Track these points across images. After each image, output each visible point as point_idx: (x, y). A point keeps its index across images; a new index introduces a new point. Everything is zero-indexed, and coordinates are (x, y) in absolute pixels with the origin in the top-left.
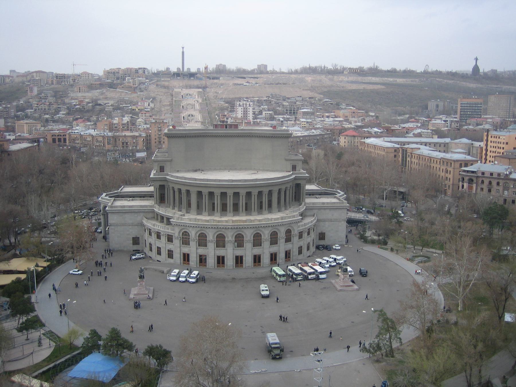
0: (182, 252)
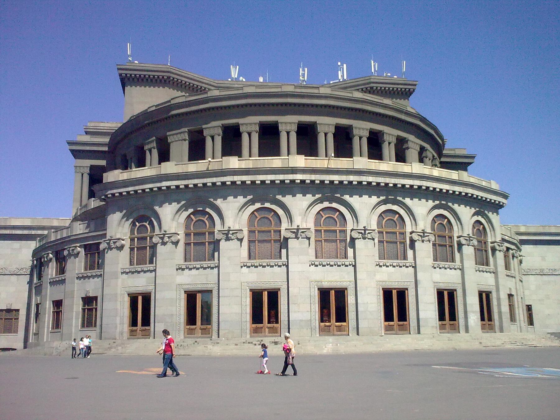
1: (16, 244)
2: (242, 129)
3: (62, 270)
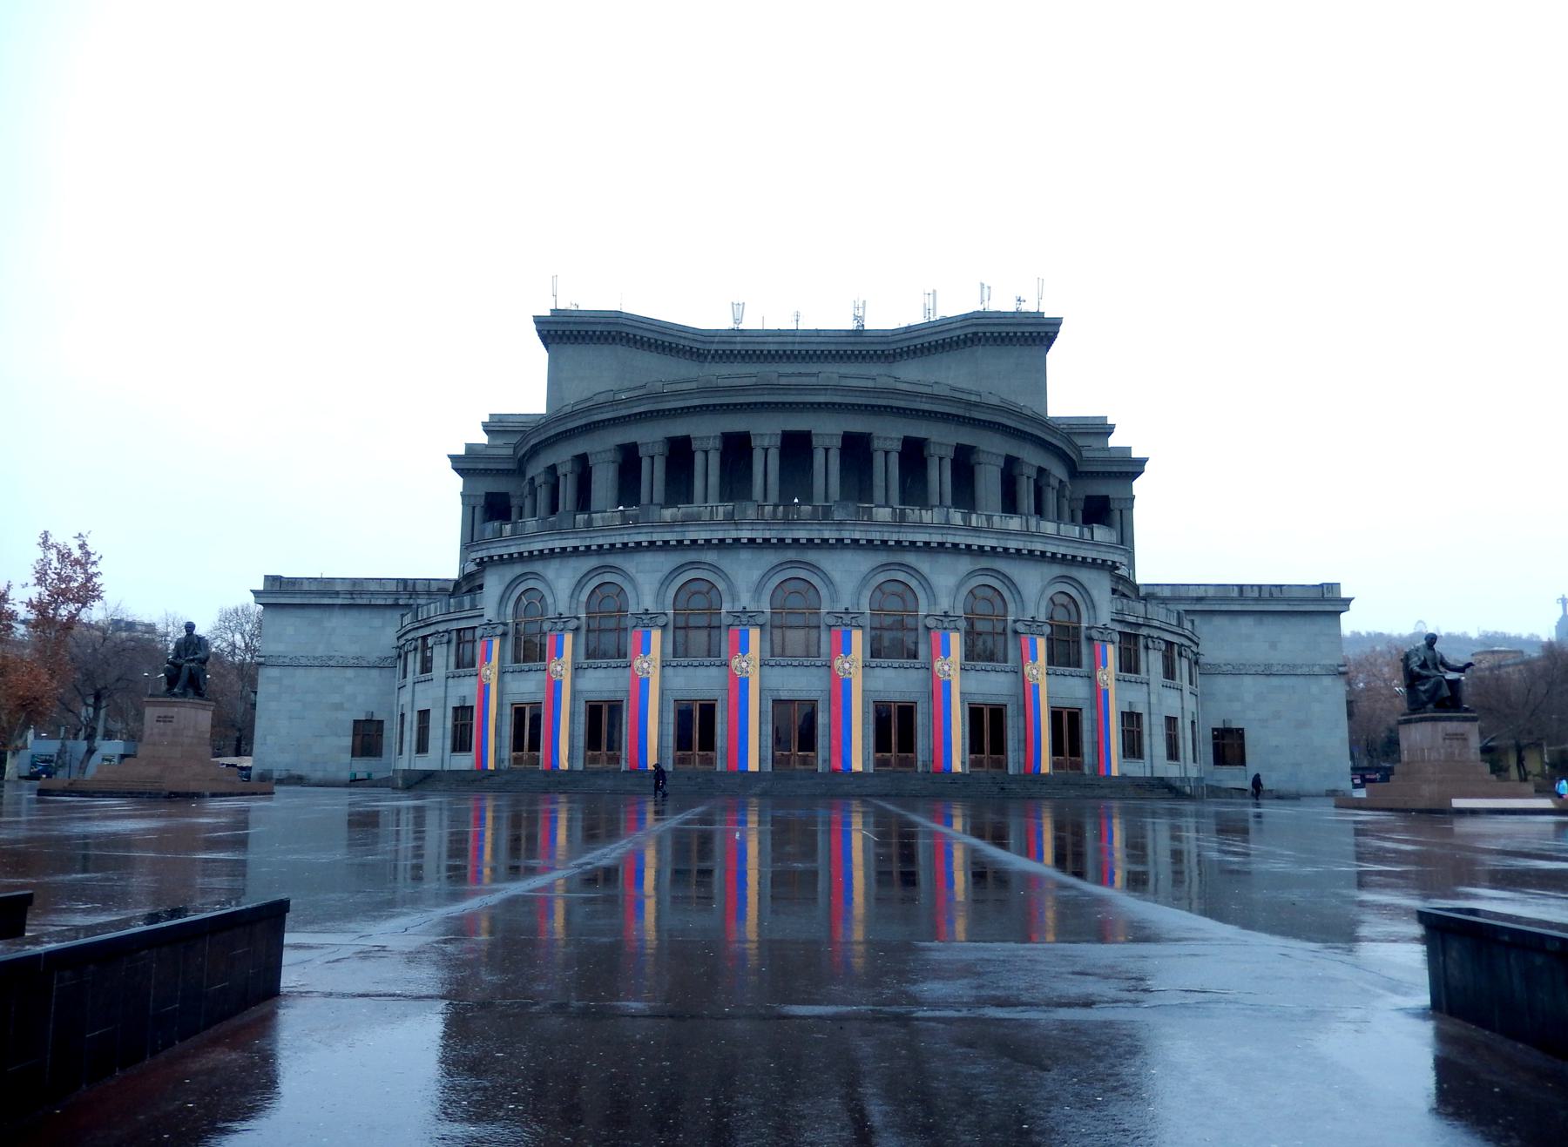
0: (508, 700)
1: (376, 620)
2: (695, 445)
3: (426, 667)
